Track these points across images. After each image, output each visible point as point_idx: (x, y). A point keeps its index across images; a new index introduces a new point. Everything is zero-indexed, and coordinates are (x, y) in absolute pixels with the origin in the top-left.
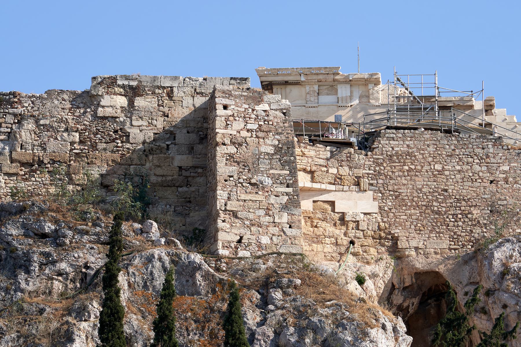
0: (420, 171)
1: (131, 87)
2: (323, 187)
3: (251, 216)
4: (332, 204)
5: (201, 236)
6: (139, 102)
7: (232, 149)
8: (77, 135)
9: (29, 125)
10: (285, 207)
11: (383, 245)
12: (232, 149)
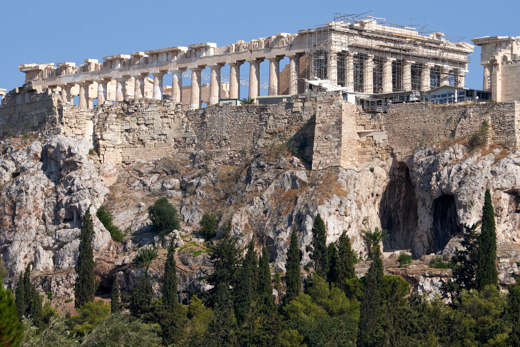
0: (401, 120)
1: (303, 98)
2: (369, 131)
3: (324, 152)
4: (372, 137)
5: (307, 162)
6: (306, 104)
7: (321, 125)
8: (286, 120)
9: (271, 118)
10: (337, 147)
11: (388, 152)
12: (321, 125)
